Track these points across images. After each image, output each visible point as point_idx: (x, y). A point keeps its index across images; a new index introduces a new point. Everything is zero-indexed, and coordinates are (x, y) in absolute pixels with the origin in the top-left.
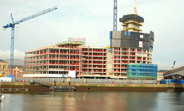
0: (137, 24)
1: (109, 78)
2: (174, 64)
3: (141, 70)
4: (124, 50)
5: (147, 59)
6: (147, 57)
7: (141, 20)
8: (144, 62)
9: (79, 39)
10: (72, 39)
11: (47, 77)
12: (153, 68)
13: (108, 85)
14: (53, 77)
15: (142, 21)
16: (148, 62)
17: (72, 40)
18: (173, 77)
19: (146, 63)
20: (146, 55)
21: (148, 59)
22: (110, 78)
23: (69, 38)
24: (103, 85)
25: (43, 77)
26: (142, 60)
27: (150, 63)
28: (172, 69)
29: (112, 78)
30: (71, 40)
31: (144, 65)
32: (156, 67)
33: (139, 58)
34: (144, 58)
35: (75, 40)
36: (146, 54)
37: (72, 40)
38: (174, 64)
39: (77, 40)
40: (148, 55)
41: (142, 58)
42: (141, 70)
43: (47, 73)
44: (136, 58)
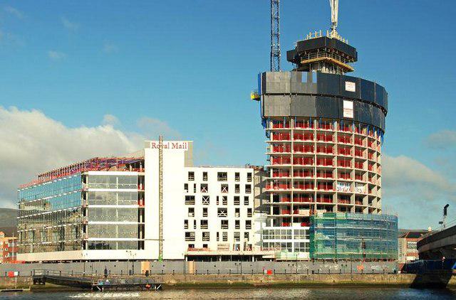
0: (338, 64)
1: (259, 258)
3: (349, 233)
4: (301, 176)
5: (366, 200)
6: (367, 194)
7: (349, 53)
8: (359, 210)
11: (84, 261)
12: (385, 227)
13: (257, 279)
14: (102, 261)
15: (350, 58)
16: (370, 210)
19: (366, 211)
20: (363, 190)
21: (371, 199)
22: (263, 259)
24: (243, 278)
25: (74, 261)
26: (353, 203)
27: (375, 212)
28: (439, 228)
29: (268, 259)
31: (357, 216)
32: (394, 223)
33: (343, 197)
34: (359, 198)
36: (364, 184)
40: (371, 187)
41: (353, 198)
42: (349, 233)
43: (85, 249)
44: (335, 197)
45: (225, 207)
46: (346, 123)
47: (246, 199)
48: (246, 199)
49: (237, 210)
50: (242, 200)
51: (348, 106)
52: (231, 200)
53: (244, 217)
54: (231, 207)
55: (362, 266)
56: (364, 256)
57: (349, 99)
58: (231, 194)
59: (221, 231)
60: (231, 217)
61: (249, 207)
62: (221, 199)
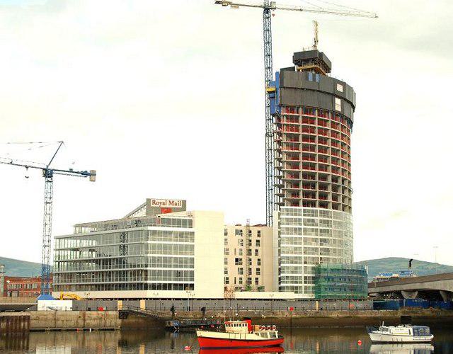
2: (410, 265)
9: (171, 203)
10: (154, 202)
17: (154, 205)
18: (404, 294)
23: (148, 200)
30: (152, 205)
35: (162, 206)
37: (154, 205)
38: (410, 265)
39: (167, 206)
45: (240, 257)
46: (336, 115)
47: (257, 251)
48: (257, 251)
49: (250, 260)
50: (253, 252)
51: (338, 101)
52: (245, 252)
53: (254, 267)
54: (244, 258)
55: (353, 304)
56: (353, 297)
57: (339, 97)
58: (244, 248)
59: (238, 276)
60: (244, 266)
61: (258, 257)
62: (238, 251)
